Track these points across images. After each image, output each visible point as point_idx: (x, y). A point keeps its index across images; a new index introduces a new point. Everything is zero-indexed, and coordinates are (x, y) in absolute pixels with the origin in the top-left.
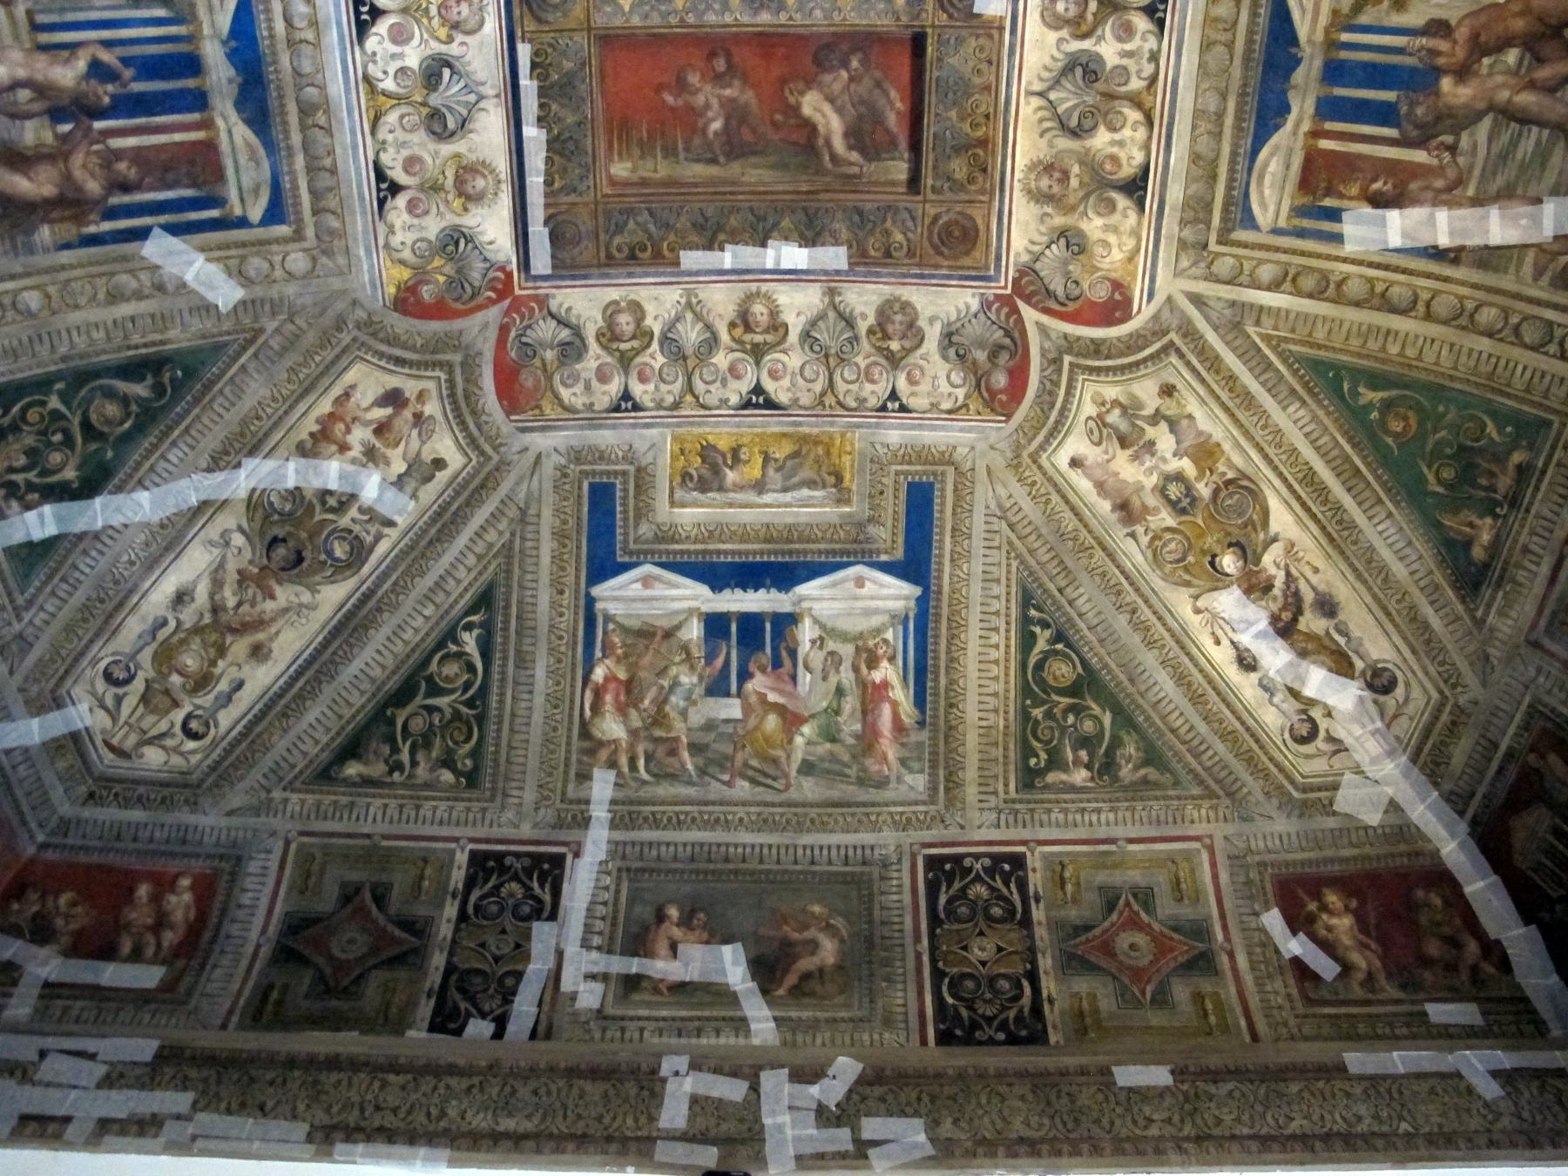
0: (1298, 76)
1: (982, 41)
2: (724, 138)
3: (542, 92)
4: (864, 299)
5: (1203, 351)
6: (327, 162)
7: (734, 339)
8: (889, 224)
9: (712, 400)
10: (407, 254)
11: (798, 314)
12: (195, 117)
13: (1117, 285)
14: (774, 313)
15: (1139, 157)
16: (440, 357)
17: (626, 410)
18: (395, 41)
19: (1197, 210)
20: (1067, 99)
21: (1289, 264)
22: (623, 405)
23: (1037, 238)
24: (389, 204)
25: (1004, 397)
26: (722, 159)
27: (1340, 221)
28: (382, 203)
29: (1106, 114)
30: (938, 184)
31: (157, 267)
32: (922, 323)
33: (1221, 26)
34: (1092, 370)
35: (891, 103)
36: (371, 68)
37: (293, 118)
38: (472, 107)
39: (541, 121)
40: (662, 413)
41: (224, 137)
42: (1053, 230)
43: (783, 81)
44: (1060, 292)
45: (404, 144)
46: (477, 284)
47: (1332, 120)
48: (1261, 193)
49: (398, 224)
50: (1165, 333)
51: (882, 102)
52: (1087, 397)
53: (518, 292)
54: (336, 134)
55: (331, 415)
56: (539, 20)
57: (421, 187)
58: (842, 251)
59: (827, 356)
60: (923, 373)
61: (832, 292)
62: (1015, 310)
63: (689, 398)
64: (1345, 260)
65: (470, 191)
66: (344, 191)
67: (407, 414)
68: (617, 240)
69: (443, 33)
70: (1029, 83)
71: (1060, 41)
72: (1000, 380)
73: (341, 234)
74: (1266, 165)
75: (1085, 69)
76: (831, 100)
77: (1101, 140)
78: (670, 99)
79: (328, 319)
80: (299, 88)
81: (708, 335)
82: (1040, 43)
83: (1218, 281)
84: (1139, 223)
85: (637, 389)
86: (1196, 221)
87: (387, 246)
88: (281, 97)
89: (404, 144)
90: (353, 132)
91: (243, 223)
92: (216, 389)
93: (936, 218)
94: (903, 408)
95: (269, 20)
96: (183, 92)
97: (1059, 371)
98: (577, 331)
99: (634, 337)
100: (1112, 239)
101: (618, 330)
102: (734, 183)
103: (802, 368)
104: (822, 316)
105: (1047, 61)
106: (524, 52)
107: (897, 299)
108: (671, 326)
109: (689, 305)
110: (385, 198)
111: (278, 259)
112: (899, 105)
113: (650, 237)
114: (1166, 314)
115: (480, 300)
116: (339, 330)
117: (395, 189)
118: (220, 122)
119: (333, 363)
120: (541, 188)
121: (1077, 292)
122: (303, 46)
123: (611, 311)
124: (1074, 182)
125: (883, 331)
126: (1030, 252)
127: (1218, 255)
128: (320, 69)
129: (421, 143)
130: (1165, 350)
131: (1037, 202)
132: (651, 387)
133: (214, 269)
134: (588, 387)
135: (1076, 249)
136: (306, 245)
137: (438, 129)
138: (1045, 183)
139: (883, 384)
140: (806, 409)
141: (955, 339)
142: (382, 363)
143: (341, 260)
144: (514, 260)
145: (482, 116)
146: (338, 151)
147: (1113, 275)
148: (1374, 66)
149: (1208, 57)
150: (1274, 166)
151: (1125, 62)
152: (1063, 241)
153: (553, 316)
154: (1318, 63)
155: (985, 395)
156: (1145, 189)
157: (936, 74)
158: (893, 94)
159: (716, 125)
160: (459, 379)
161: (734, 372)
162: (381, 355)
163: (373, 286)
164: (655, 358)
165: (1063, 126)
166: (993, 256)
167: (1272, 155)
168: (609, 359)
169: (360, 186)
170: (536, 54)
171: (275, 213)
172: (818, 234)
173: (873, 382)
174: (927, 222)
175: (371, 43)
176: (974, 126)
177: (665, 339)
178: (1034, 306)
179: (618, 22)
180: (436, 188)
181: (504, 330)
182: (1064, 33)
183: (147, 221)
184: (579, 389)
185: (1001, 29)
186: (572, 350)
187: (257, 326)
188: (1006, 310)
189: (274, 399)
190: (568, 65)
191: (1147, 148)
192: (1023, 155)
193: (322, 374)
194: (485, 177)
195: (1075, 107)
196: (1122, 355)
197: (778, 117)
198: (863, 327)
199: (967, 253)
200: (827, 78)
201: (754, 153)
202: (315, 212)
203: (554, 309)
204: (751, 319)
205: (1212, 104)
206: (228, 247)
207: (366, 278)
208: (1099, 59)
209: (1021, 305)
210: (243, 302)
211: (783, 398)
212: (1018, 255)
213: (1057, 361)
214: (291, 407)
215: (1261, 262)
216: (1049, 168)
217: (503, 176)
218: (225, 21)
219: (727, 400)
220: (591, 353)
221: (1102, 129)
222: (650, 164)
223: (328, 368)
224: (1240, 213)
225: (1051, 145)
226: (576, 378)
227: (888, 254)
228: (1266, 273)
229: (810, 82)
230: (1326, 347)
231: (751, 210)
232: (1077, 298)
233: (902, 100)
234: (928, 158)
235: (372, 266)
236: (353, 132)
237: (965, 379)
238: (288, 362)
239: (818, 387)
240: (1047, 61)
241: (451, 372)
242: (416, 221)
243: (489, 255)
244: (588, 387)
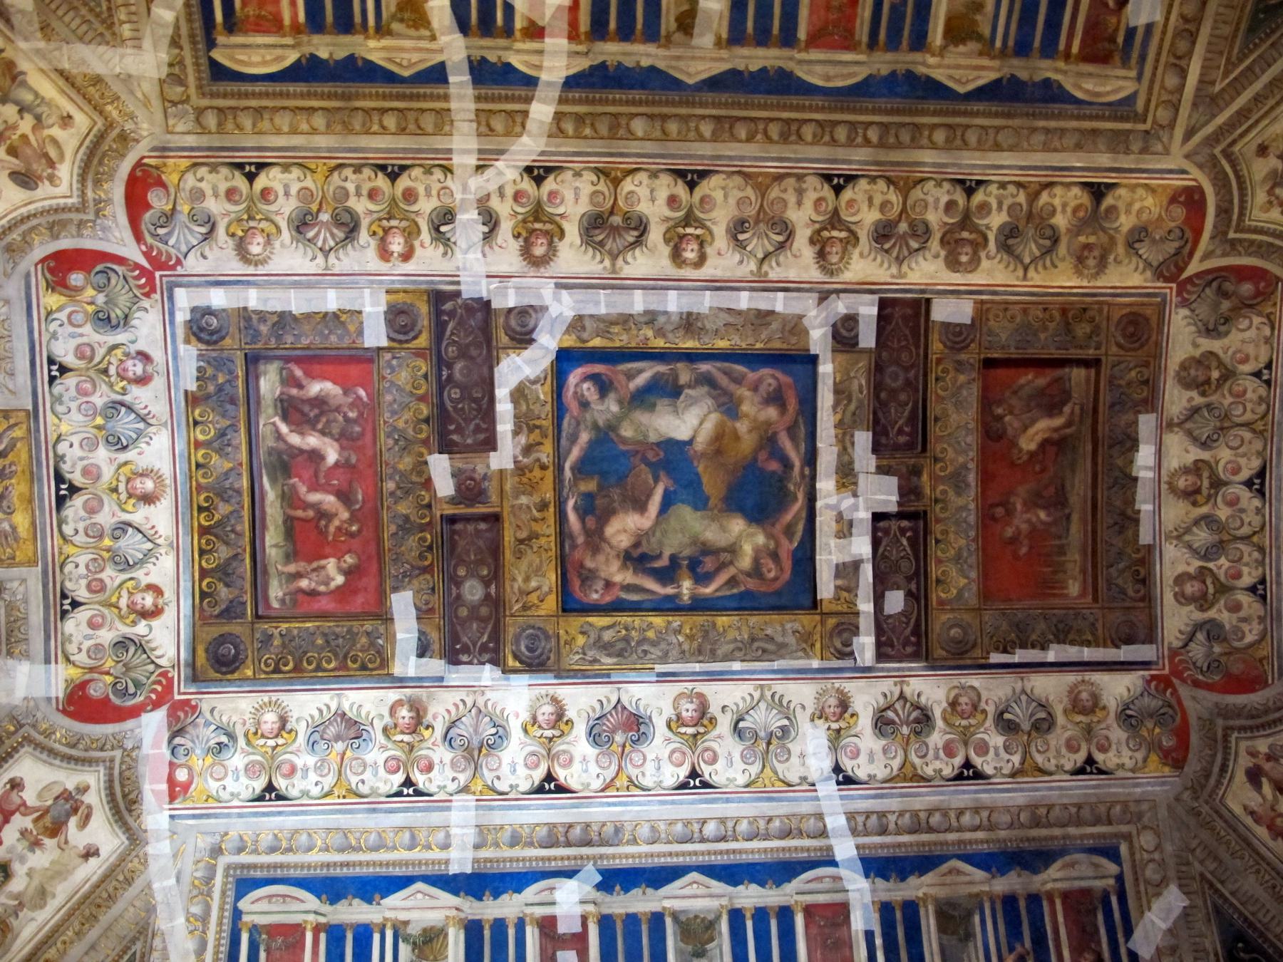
0: (1023, 75)
1: (991, 317)
2: (1052, 510)
3: (1023, 646)
4: (1176, 399)
5: (1231, 125)
6: (1073, 810)
7: (1206, 503)
8: (1123, 382)
9: (1257, 521)
10: (1139, 756)
11: (1187, 451)
12: (1045, 904)
13: (1173, 200)
14: (1186, 470)
15: (1076, 191)
16: (1220, 733)
17: (1265, 590)
18: (987, 752)
19: (1118, 142)
20: (1030, 249)
21: (1167, 63)
22: (1261, 592)
23: (1133, 266)
24: (1103, 768)
25: (1262, 284)
26: (1067, 511)
27: (1135, 29)
28: (1101, 772)
29: (1042, 218)
30: (1093, 344)
31: (1157, 948)
32: (1197, 353)
33: (984, 137)
34: (1241, 214)
35: (1029, 382)
36: (1006, 771)
37: (1044, 832)
38: (1031, 699)
39: (1044, 648)
40: (1267, 561)
41: (1059, 885)
42: (1127, 253)
43: (1013, 465)
44: (1176, 244)
45: (1058, 752)
46: (1160, 703)
47: (1057, 44)
48: (1108, 93)
49: (1116, 761)
50: (1214, 157)
51: (1027, 391)
52: (1264, 216)
53: (1166, 671)
54: (1053, 801)
55: (1270, 828)
56: (974, 646)
57: (1089, 741)
58: (1143, 418)
59: (1222, 429)
60: (1240, 351)
61: (1170, 425)
62: (1190, 280)
63: (1255, 539)
64: (1167, 19)
65: (1090, 703)
66: (1093, 800)
67: (1267, 766)
68: (1131, 592)
69: (980, 717)
70: (1018, 279)
71: (988, 257)
72: (1247, 288)
73: (1125, 804)
74: (1087, 92)
75: (1009, 236)
76: (1025, 428)
77: (1061, 221)
78: (1024, 550)
79: (1192, 822)
80: (1022, 826)
81: (1202, 523)
82: (990, 272)
83: (1175, 119)
84: (1125, 186)
85: (1247, 580)
86: (1127, 142)
87: (1133, 771)
88: (1028, 840)
89: (1058, 752)
90: (1051, 789)
91: (1120, 878)
92: (1251, 917)
93: (1119, 346)
94: (1269, 366)
95: (976, 842)
96: (1029, 912)
97: (1240, 241)
98: (1198, 627)
99: (1204, 582)
100: (1137, 206)
101: (1197, 594)
102: (1085, 502)
103: (1231, 448)
104: (1189, 433)
105: (1001, 266)
106: (996, 658)
107: (1178, 373)
108: (1195, 552)
109: (1178, 537)
110: (1097, 769)
111: (1146, 856)
112: (1030, 377)
113: (1129, 567)
114: (1199, 158)
115: (1174, 702)
116: (1199, 814)
117: (1090, 761)
118: (1049, 886)
119: (1226, 821)
120: (1093, 650)
121: (1178, 232)
122: (992, 819)
123: (1182, 598)
124: (1092, 239)
125: (1202, 384)
126: (1144, 270)
127: (1154, 122)
128: (1007, 809)
129: (1057, 738)
130: (1227, 154)
131: (1105, 267)
132: (1245, 570)
133: (1157, 905)
134: (1244, 620)
135: (1143, 234)
136: (1134, 832)
137: (1045, 726)
138: (1091, 262)
139: (1247, 383)
140: (1265, 445)
141: (1211, 327)
142: (1226, 782)
143: (1145, 807)
144: (1142, 673)
145: (1036, 691)
146: (1065, 801)
147: (1165, 203)
148: (1021, 20)
149: (1005, 146)
150: (1089, 85)
151: (1005, 207)
152: (1137, 245)
153: (1186, 645)
154: (1016, 62)
155: (1259, 299)
156: (1099, 184)
157: (1013, 350)
158: (1022, 381)
159: (1043, 515)
160: (1238, 722)
161: (1233, 503)
162: (1219, 783)
163: (1163, 784)
164: (1221, 565)
165: (1048, 251)
166: (1145, 300)
167: (1080, 88)
168: (1222, 602)
169: (1087, 787)
170: (997, 649)
171: (1112, 854)
172: (1129, 437)
173: (1245, 392)
174: (1122, 353)
175: (989, 770)
176: (1052, 319)
177: (1205, 557)
178: (1187, 264)
179: (974, 587)
180: (1089, 731)
181: (1197, 684)
182: (983, 255)
183: (1123, 951)
184: (1246, 627)
185: (982, 302)
186: (1213, 631)
187: (1198, 878)
188: (1189, 287)
189: (1258, 872)
190: (1005, 626)
191: (1068, 186)
192: (1069, 279)
193: (1235, 830)
194: (1080, 692)
195: (1036, 242)
196: (1231, 193)
197: (1038, 468)
198: (1199, 400)
199: (1147, 320)
200: (1010, 431)
201: (1063, 486)
202: (1110, 823)
203: (1180, 644)
204: (1190, 489)
205: (1039, 138)
206: (1138, 892)
207: (1158, 788)
208: (1001, 228)
209: (1185, 275)
210: (1180, 886)
211: (1256, 463)
212: (1146, 280)
213: (1233, 243)
214: (1263, 858)
215: (1163, 87)
216: (1080, 260)
217: (1080, 678)
218: (979, 874)
219: (1257, 508)
220: (1216, 616)
221: (1054, 221)
222: (1070, 566)
223: (1230, 826)
224: (1123, 108)
225: (1063, 259)
226: (1237, 629)
227: (1146, 382)
228: (1172, 81)
229: (1013, 444)
230: (1238, 24)
231: (1110, 488)
232: (1182, 230)
233: (1026, 374)
234: (1075, 353)
235: (1148, 783)
236: (1051, 789)
237: (1245, 317)
238: (1225, 855)
239: (1247, 435)
240: (1001, 266)
241: (1232, 728)
242: (1114, 747)
243: (1139, 690)
244: (1244, 620)
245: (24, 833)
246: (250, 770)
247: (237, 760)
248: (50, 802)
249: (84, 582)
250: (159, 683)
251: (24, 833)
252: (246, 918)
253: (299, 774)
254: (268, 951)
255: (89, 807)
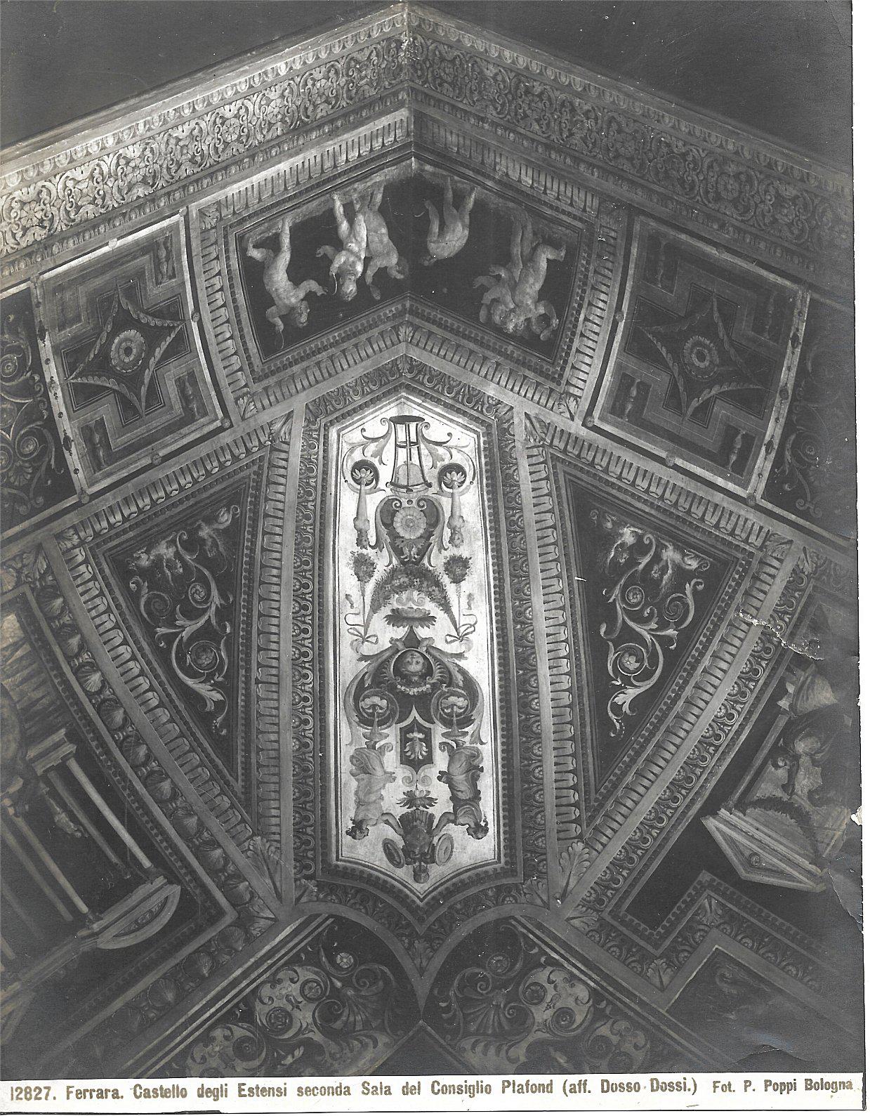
245: (431, 802)
246: (283, 1018)
247: (305, 1016)
248: (435, 840)
249: (615, 1039)
250: (450, 1021)
251: (431, 802)
252: (160, 881)
253: (230, 1051)
254: (113, 867)
255: (399, 865)
